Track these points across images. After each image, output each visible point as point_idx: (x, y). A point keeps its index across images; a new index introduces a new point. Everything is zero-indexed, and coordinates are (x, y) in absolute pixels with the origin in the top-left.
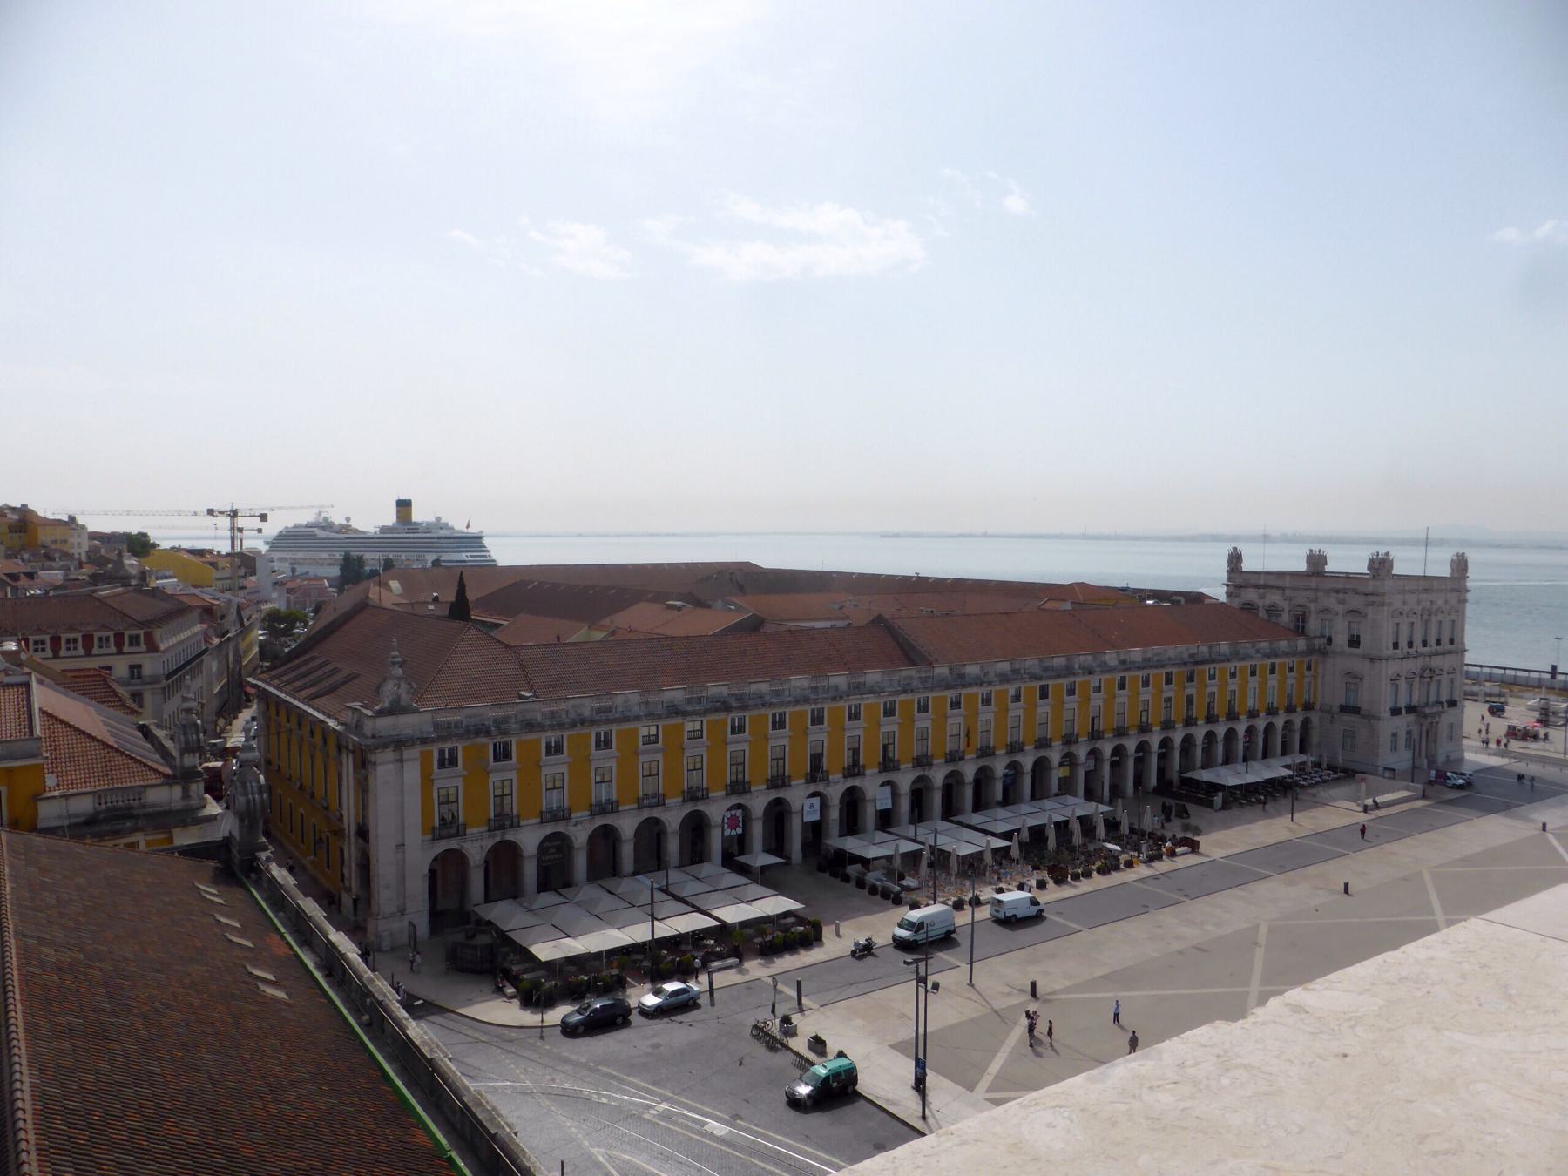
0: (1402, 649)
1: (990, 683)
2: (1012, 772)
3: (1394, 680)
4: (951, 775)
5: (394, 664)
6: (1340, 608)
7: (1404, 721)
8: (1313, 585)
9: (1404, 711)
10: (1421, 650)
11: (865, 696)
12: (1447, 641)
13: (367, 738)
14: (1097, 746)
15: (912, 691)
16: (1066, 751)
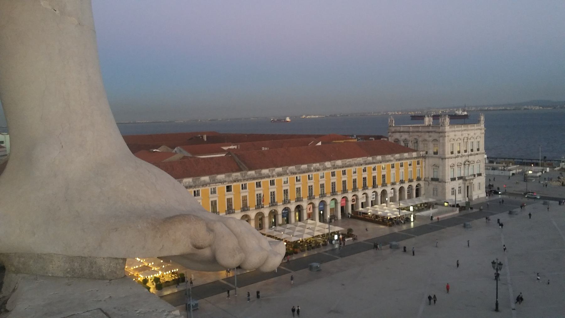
0: (455, 154)
1: (273, 176)
2: (287, 211)
3: (452, 166)
4: (258, 214)
6: (431, 139)
7: (457, 184)
8: (420, 130)
9: (457, 179)
10: (464, 154)
11: (217, 184)
12: (476, 150)
14: (323, 199)
15: (238, 181)
16: (310, 202)
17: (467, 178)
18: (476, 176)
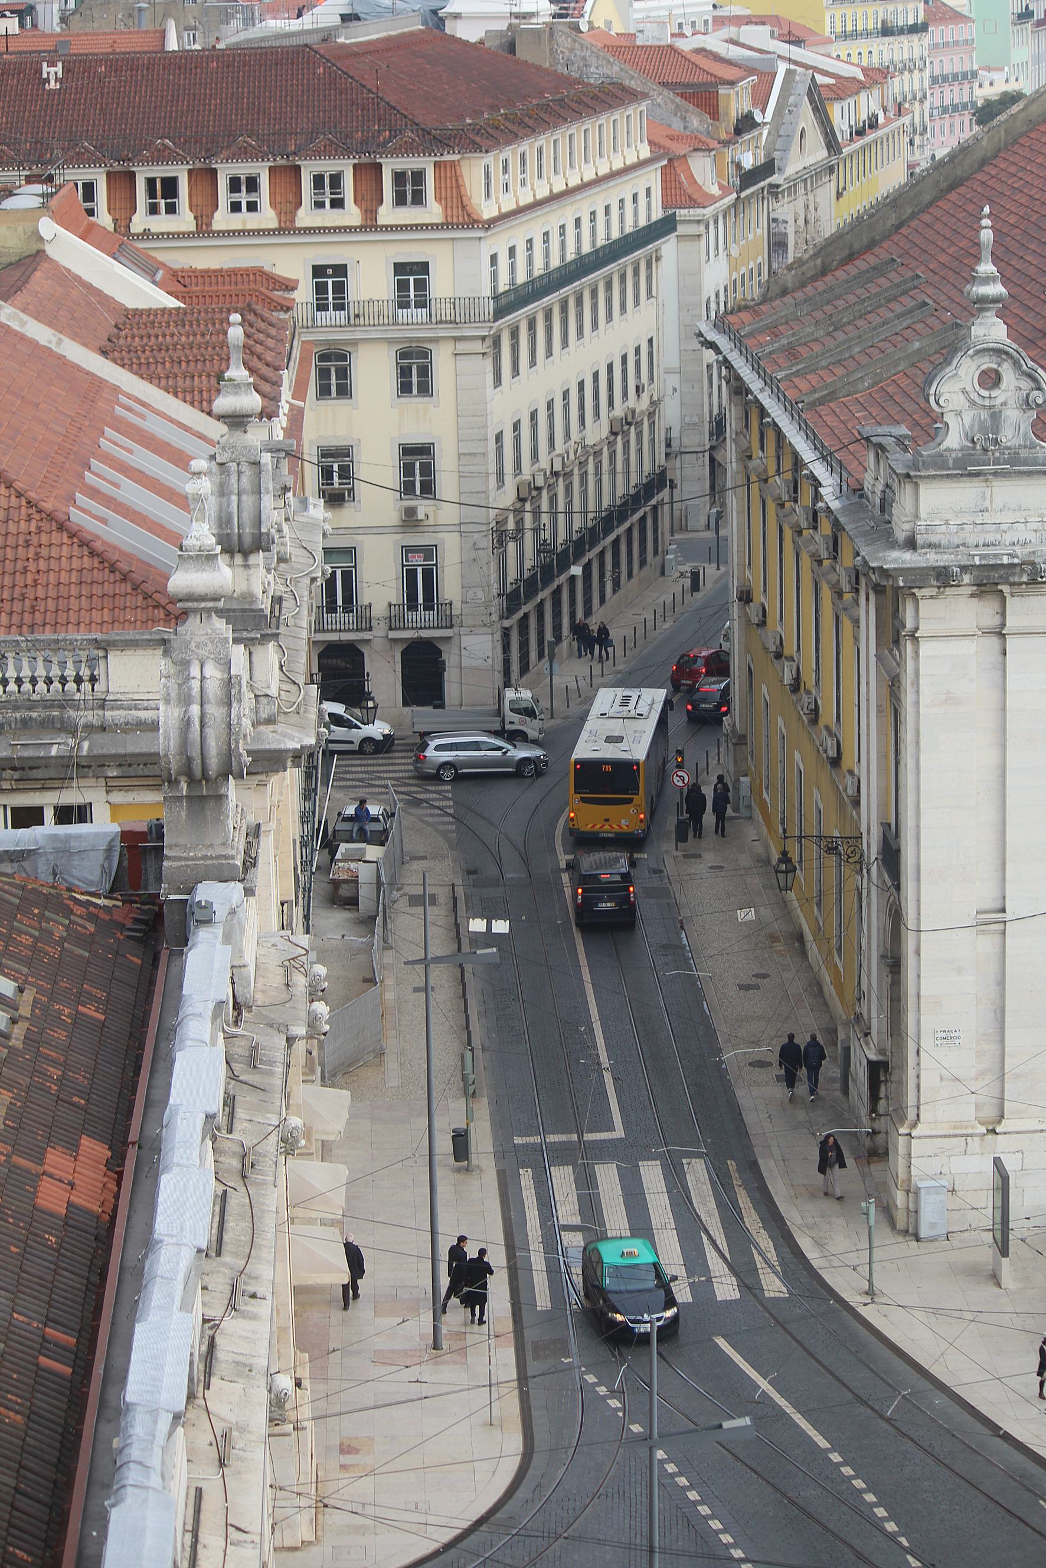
5: (984, 302)
13: (893, 545)
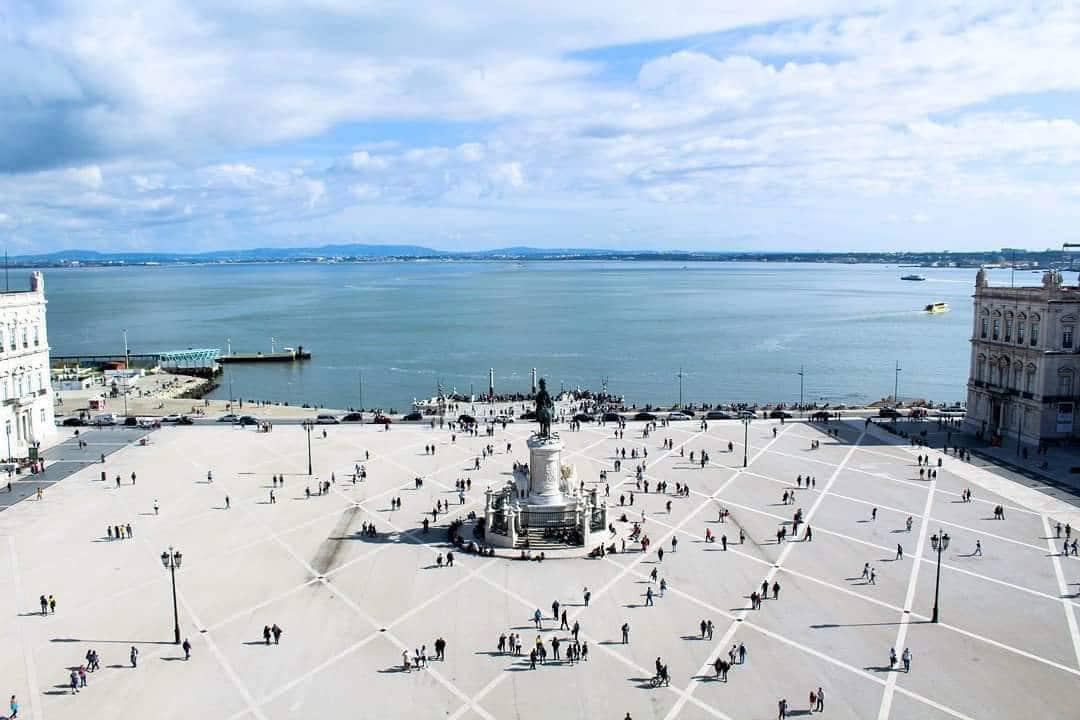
17: (21, 402)
18: (37, 394)
